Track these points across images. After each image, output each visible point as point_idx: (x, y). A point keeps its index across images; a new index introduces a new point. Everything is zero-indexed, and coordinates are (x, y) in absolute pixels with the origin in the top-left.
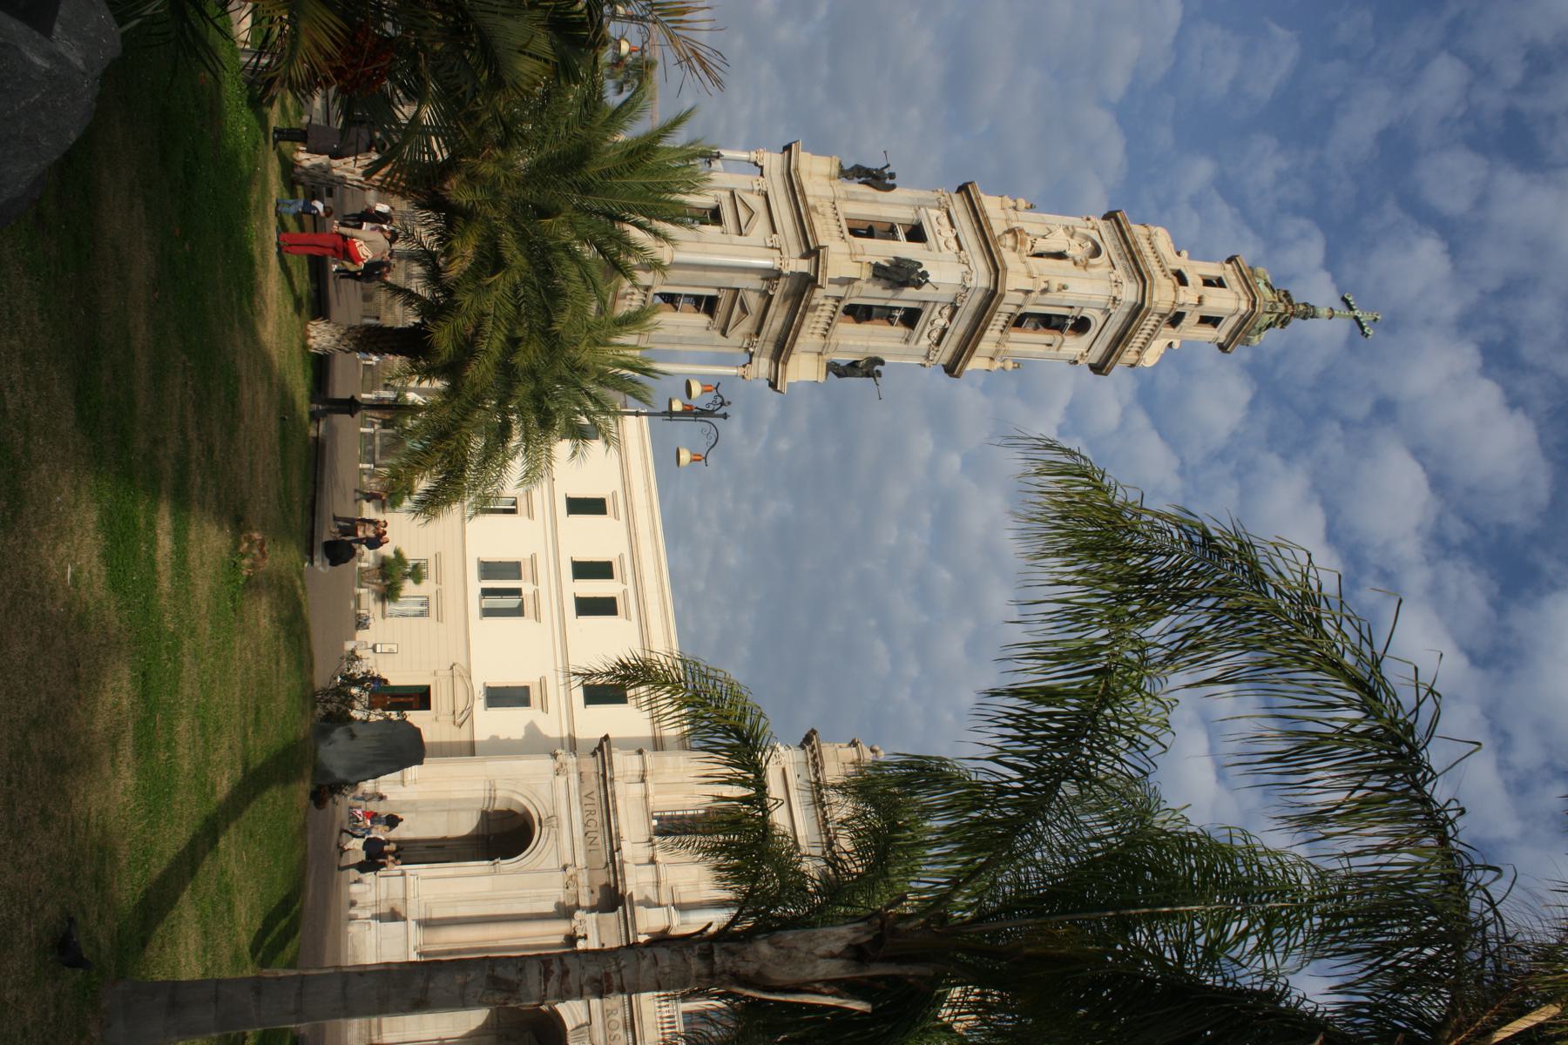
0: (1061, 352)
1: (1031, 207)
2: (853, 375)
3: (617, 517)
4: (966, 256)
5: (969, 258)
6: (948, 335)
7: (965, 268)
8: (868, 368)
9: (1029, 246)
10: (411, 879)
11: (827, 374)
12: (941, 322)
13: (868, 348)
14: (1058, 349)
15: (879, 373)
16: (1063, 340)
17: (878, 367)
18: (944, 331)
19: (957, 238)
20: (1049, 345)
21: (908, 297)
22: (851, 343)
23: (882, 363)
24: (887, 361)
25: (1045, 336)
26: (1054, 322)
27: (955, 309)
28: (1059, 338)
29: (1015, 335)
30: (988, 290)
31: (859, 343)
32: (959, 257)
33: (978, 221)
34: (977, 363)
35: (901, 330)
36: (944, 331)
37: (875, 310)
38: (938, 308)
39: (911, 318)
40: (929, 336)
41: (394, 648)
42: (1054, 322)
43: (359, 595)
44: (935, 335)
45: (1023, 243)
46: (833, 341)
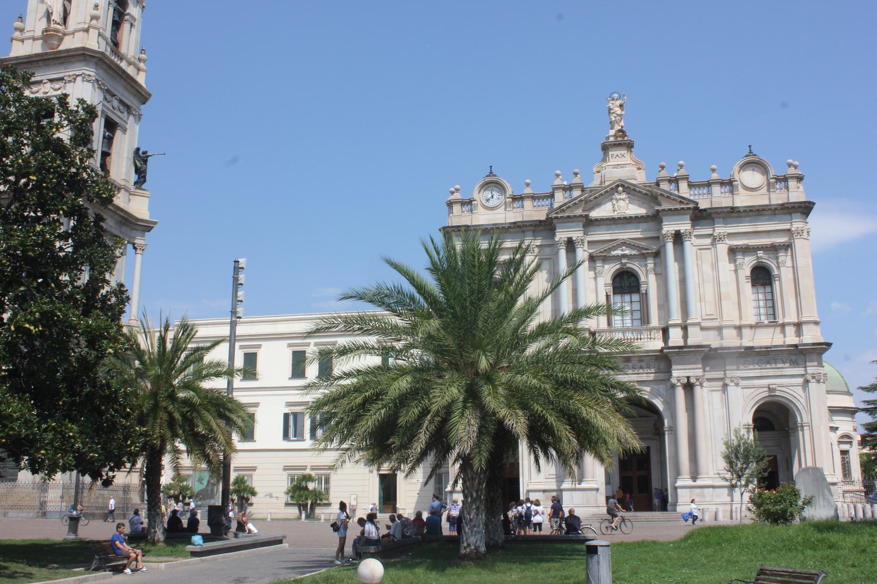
0: (136, 17)
1: (21, 18)
2: (145, 172)
3: (259, 346)
4: (69, 76)
5: (71, 73)
6: (123, 99)
7: (79, 79)
8: (141, 160)
9: (59, 27)
10: (531, 487)
11: (144, 190)
12: (116, 103)
13: (128, 158)
14: (135, 19)
15: (144, 153)
16: (128, 14)
17: (141, 152)
18: (121, 102)
19: (51, 81)
20: (132, 25)
21: (98, 127)
22: (124, 170)
23: (138, 149)
24: (136, 147)
25: (126, 26)
26: (117, 19)
27: (108, 91)
28: (127, 17)
29: (123, 50)
30: (96, 64)
31: (124, 164)
32: (70, 81)
33: (37, 61)
34: (141, 79)
35: (118, 133)
36: (121, 102)
37: (104, 149)
38: (106, 103)
39: (111, 126)
40: (123, 113)
41: (353, 497)
42: (117, 19)
43: (272, 520)
44: (121, 107)
45: (57, 31)
46: (122, 183)
